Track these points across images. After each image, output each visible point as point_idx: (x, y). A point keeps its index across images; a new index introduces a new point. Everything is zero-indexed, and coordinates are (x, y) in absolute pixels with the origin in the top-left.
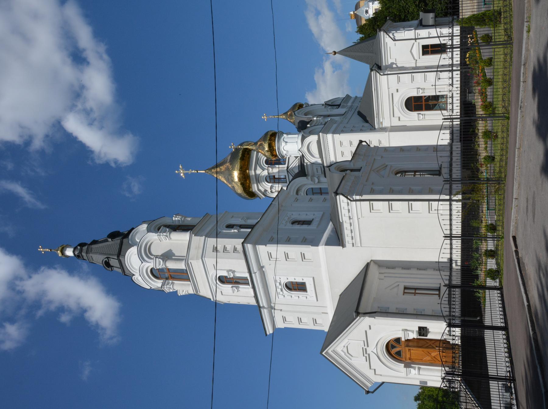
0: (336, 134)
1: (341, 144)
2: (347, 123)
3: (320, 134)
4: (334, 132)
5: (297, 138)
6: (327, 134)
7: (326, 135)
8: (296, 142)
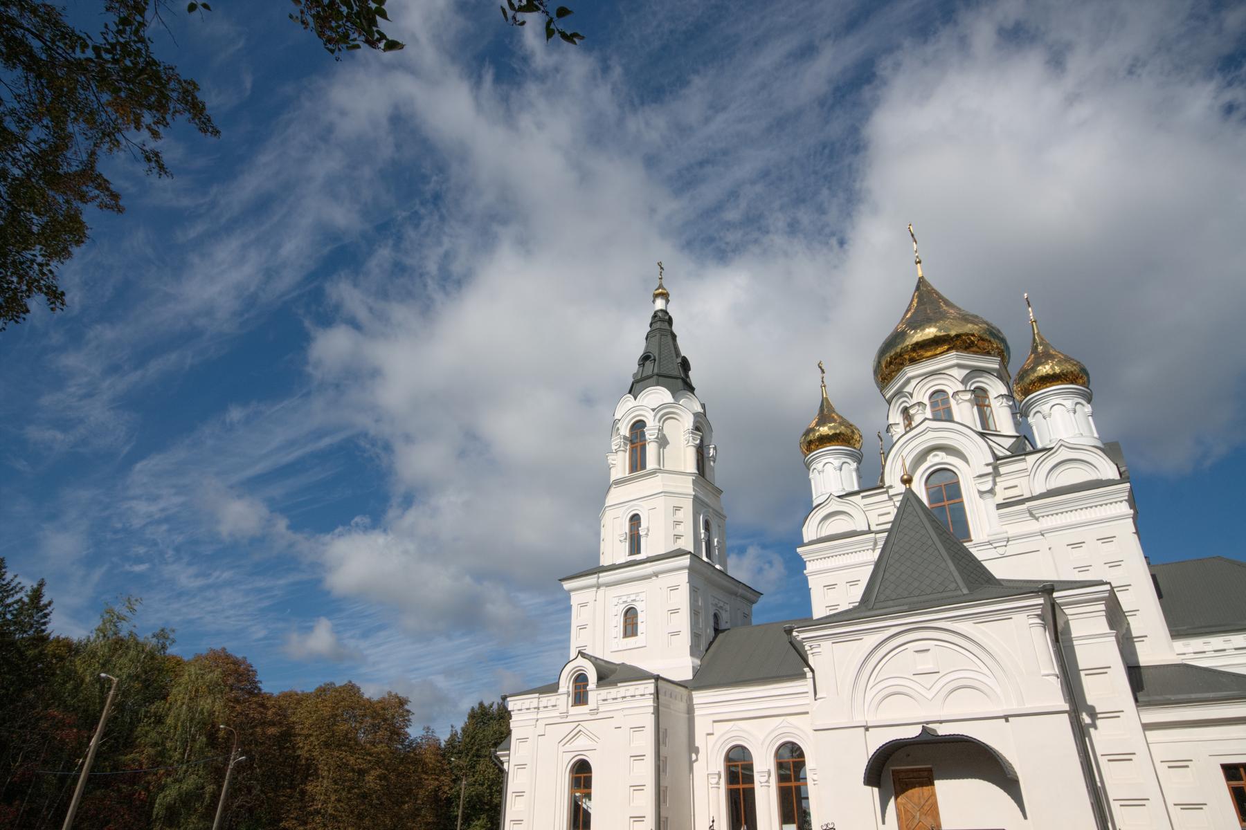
6: (1127, 504)
7: (1126, 498)
8: (1082, 434)
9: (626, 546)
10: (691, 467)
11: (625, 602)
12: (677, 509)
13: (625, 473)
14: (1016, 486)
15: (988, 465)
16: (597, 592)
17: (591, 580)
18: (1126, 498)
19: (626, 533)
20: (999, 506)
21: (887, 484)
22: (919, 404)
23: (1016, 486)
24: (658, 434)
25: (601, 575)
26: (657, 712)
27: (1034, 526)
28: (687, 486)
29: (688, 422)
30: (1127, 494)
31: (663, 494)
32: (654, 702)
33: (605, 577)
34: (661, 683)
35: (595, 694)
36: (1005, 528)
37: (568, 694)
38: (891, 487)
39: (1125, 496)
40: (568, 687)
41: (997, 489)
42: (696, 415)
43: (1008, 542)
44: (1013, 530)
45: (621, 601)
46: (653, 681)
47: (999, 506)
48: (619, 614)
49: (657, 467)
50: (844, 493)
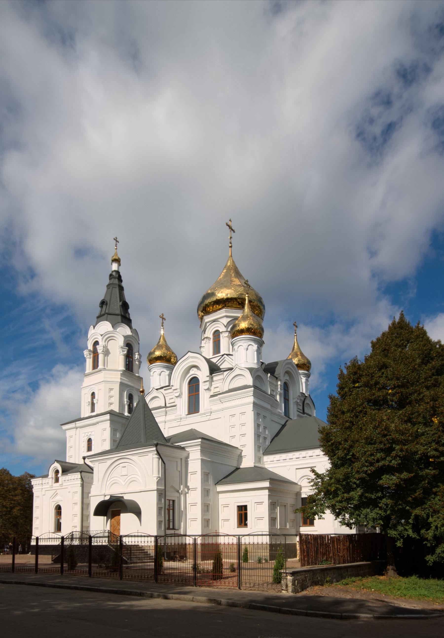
0: (253, 406)
1: (243, 413)
2: (272, 420)
3: (253, 388)
4: (255, 404)
5: (253, 363)
8: (247, 362)
9: (90, 407)
10: (121, 366)
11: (87, 435)
12: (111, 389)
13: (90, 370)
14: (218, 387)
15: (207, 376)
16: (76, 431)
17: (72, 425)
18: (252, 394)
19: (89, 402)
20: (212, 396)
21: (171, 385)
22: (207, 338)
23: (218, 387)
24: (103, 349)
25: (77, 423)
26: (82, 486)
27: (221, 406)
28: (117, 378)
29: (121, 341)
30: (252, 393)
31: (103, 382)
32: (81, 482)
33: (79, 424)
34: (83, 473)
35: (62, 478)
36: (212, 407)
37: (52, 478)
38: (172, 386)
39: (252, 393)
40: (52, 475)
41: (212, 388)
42: (126, 337)
43: (211, 413)
44: (214, 408)
45: (85, 435)
46: (79, 473)
47: (212, 396)
48: (85, 440)
49: (103, 367)
50: (159, 387)
